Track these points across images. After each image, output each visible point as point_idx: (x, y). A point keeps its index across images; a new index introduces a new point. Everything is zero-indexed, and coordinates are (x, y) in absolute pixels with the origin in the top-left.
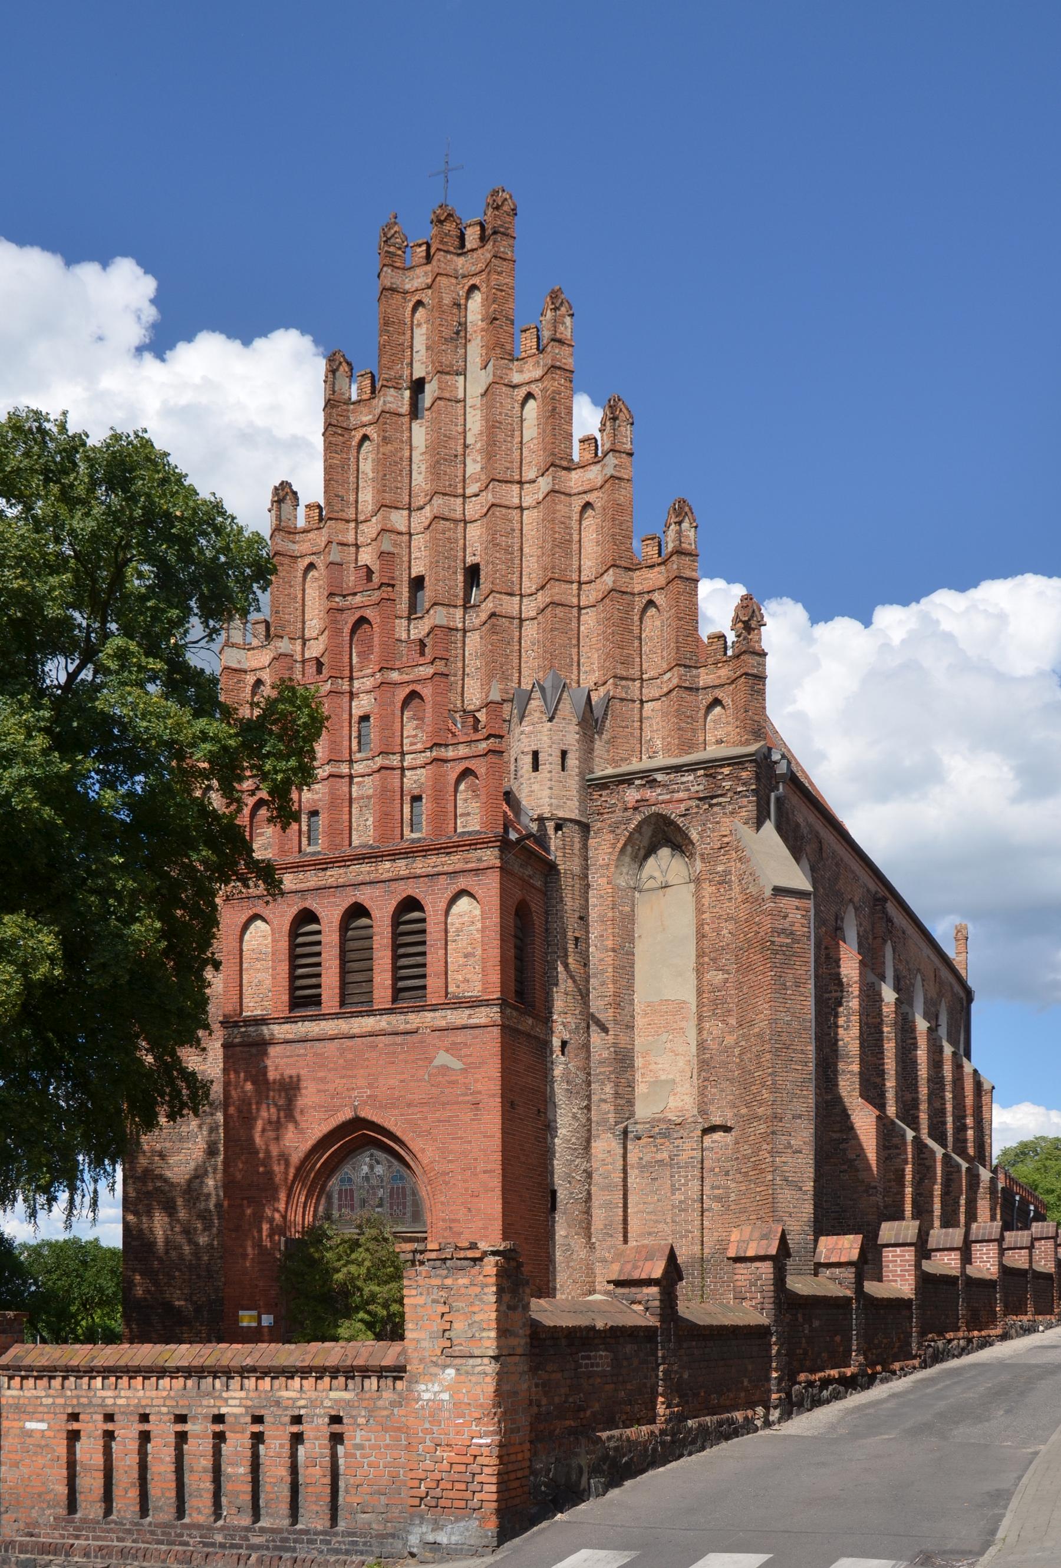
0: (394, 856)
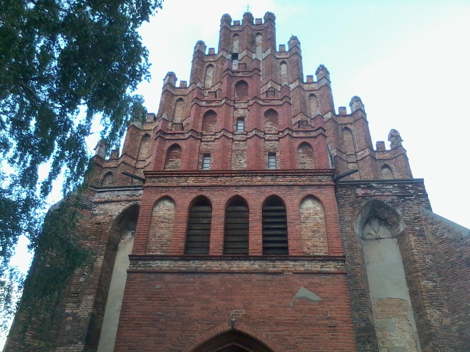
0: (264, 173)
